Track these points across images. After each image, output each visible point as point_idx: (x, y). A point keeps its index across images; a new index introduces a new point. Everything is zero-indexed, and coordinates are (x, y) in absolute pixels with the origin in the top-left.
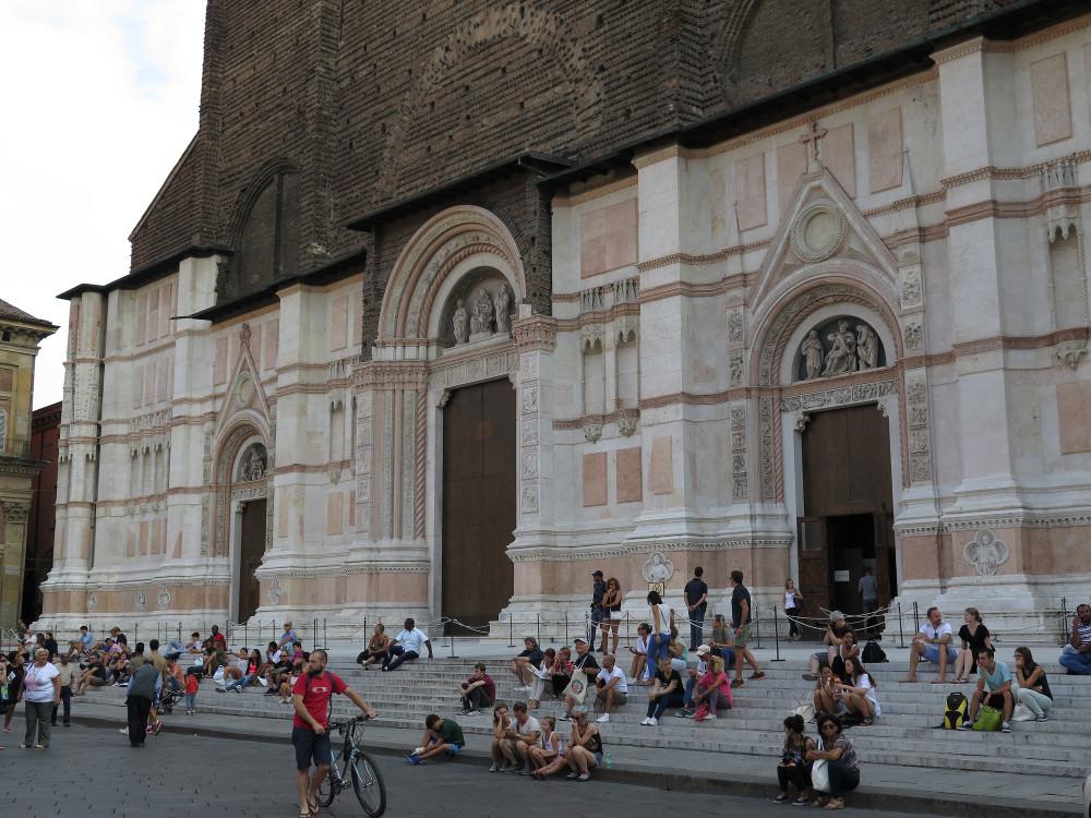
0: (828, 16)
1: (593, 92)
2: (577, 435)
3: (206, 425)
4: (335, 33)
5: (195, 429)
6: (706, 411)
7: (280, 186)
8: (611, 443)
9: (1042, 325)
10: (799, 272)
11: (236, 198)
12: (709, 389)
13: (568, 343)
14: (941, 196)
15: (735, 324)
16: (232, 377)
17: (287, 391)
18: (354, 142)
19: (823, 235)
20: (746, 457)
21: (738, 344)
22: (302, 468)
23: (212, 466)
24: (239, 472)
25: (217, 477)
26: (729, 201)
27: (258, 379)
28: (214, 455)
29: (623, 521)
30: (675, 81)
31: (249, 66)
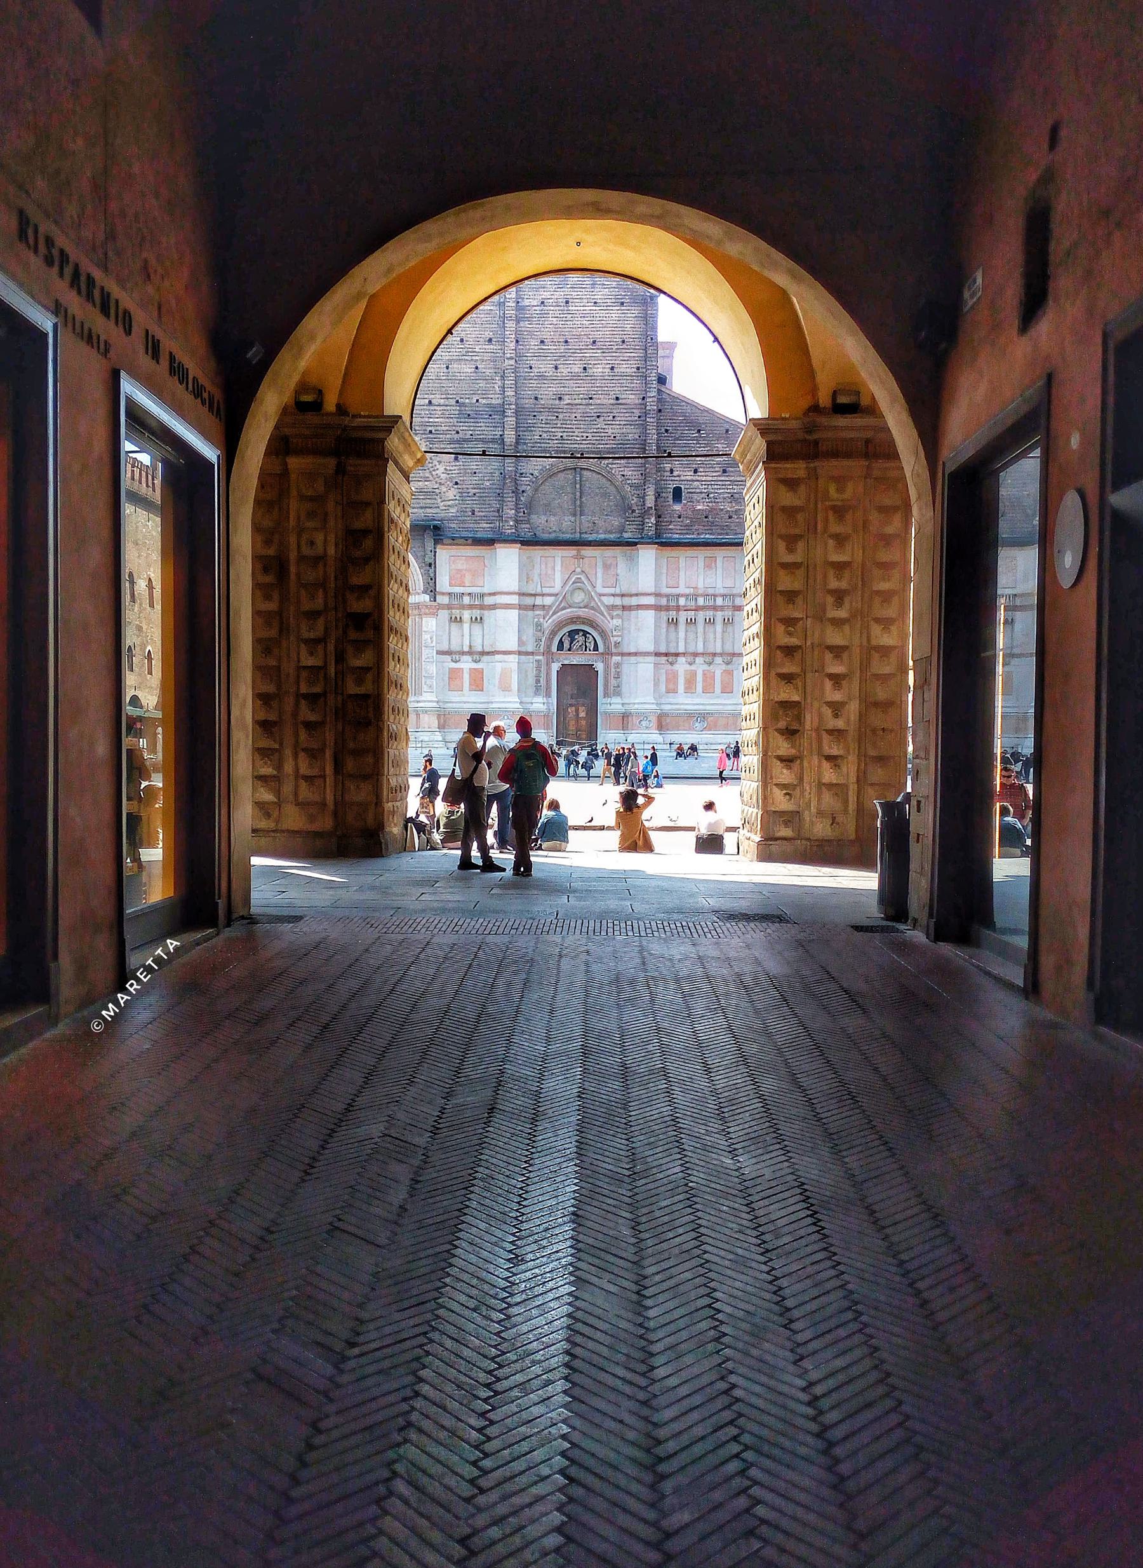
0: (578, 503)
1: (452, 493)
2: (448, 658)
6: (523, 657)
8: (466, 664)
9: (663, 650)
10: (569, 610)
12: (523, 649)
13: (444, 614)
14: (631, 596)
15: (538, 626)
19: (579, 597)
20: (541, 679)
21: (539, 634)
26: (536, 571)
29: (473, 699)
30: (513, 511)
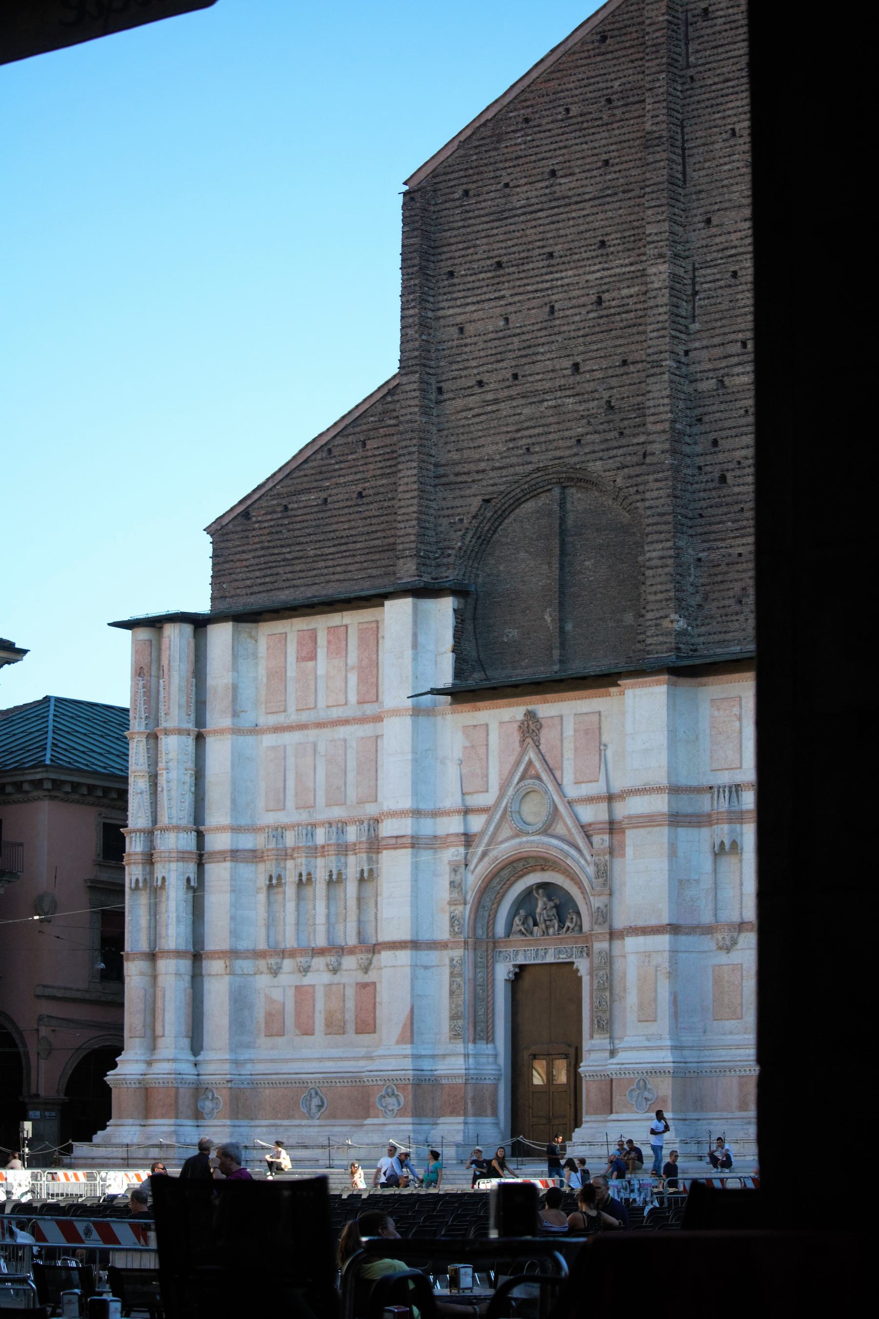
3: (452, 850)
4: (685, 309)
5: (425, 856)
7: (562, 504)
11: (474, 510)
16: (503, 789)
17: (648, 821)
18: (729, 475)
22: (674, 929)
23: (465, 912)
24: (510, 925)
25: (475, 928)
27: (563, 795)
28: (470, 897)
31: (498, 311)
